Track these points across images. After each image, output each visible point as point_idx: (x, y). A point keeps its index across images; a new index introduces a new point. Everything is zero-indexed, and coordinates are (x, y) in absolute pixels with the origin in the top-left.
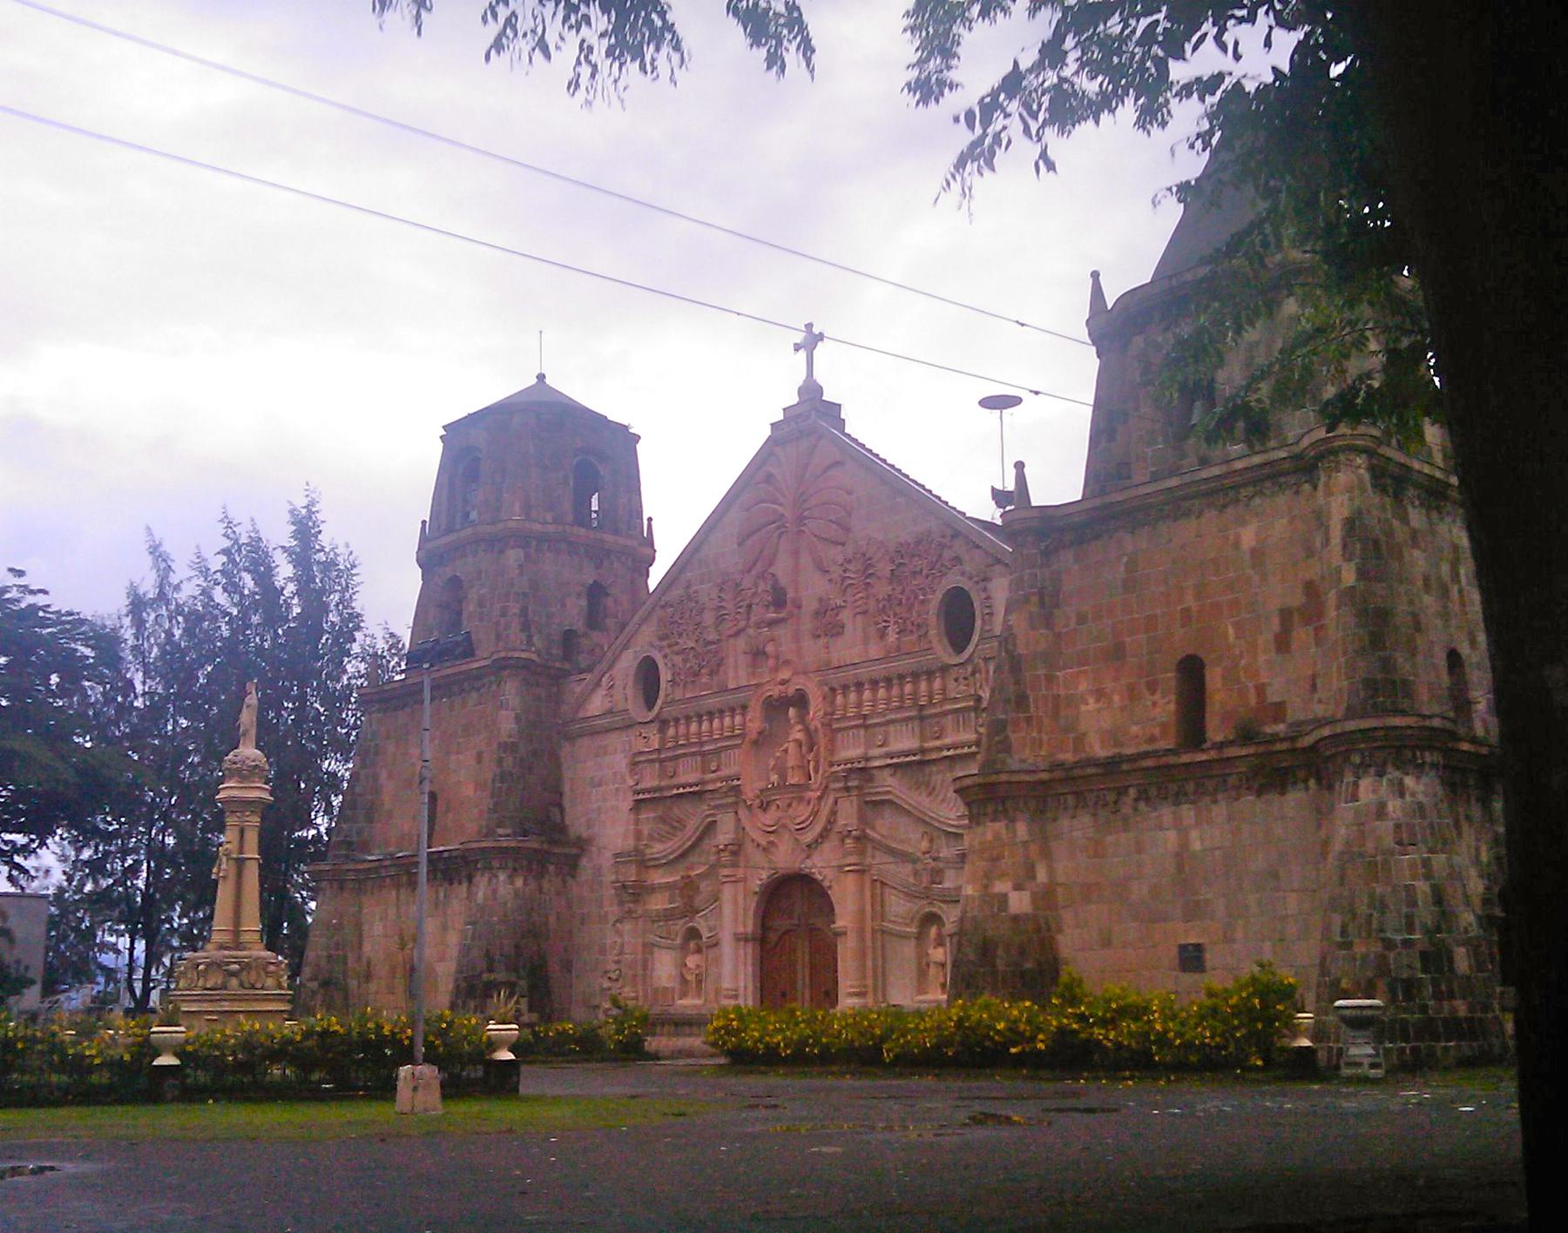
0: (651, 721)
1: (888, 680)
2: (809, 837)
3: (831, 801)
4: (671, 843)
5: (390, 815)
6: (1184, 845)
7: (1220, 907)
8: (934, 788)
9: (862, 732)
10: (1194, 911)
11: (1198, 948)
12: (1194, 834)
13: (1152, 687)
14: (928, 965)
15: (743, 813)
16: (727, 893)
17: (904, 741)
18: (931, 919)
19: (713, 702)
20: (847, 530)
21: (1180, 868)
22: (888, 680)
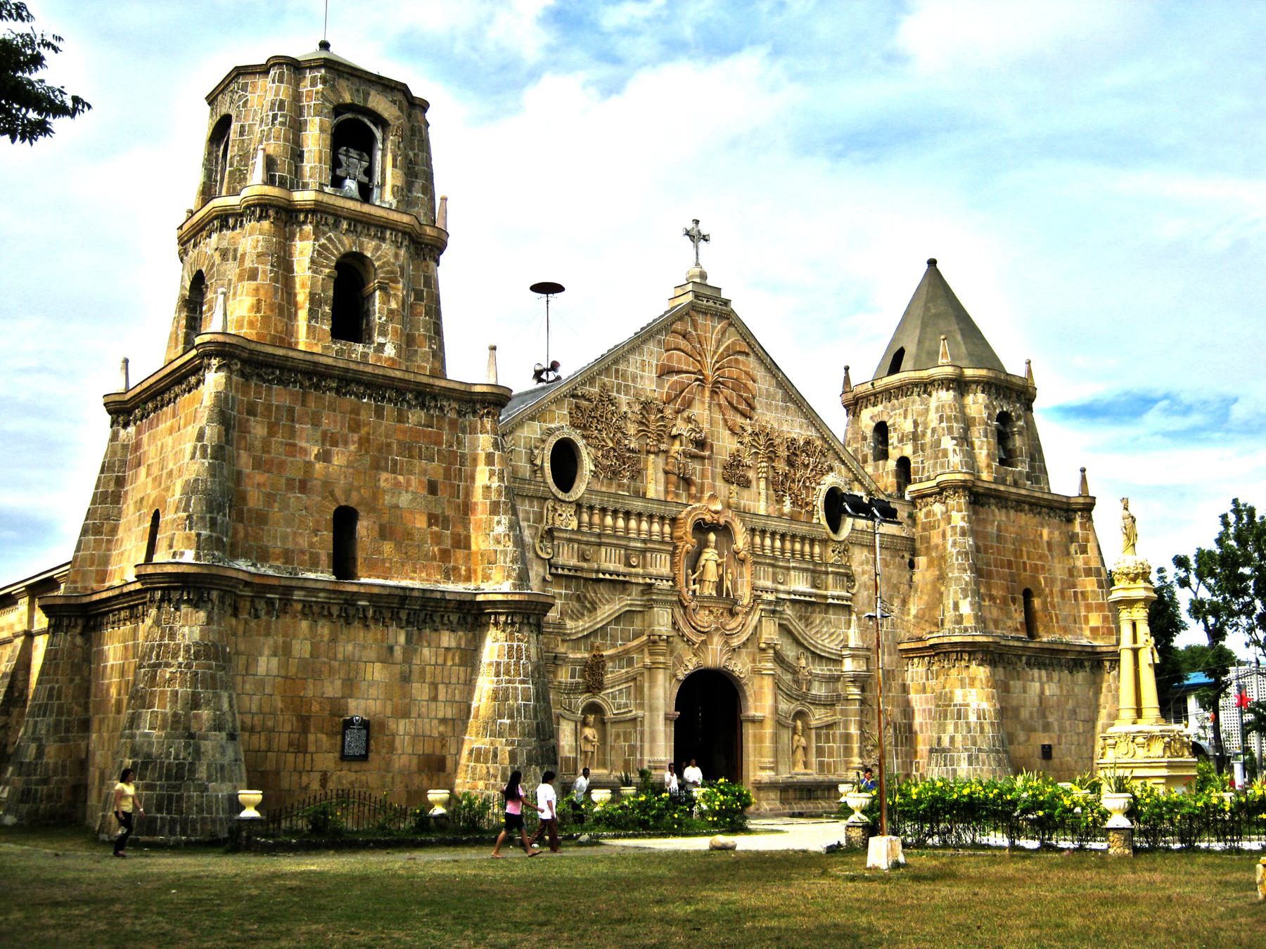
0: (570, 503)
1: (783, 536)
2: (735, 642)
3: (757, 617)
4: (581, 623)
5: (262, 518)
6: (1042, 692)
7: (1056, 725)
8: (811, 623)
9: (771, 569)
10: (1047, 728)
11: (1050, 746)
12: (1046, 687)
13: (1014, 600)
14: (798, 747)
15: (679, 612)
16: (661, 677)
17: (800, 584)
18: (800, 715)
19: (638, 505)
20: (752, 408)
21: (1041, 703)
22: (783, 536)
